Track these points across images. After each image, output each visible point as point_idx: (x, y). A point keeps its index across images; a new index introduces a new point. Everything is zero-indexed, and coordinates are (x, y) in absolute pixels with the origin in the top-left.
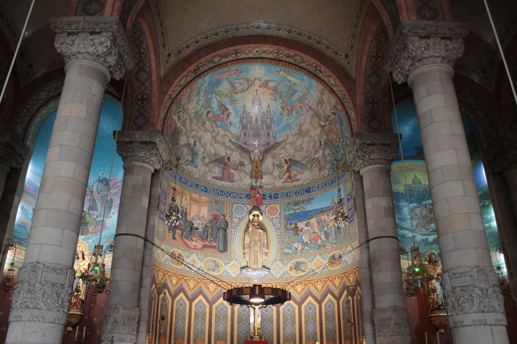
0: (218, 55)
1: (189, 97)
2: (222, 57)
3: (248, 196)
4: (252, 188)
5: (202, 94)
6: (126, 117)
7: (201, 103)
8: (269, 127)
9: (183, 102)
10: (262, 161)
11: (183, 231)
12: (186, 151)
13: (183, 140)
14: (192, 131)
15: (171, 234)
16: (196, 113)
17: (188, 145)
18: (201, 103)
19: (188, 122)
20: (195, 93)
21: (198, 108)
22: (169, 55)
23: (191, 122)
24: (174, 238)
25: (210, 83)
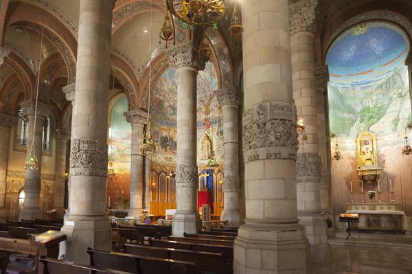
0: (162, 62)
1: (161, 84)
2: (165, 62)
3: (204, 124)
4: (206, 120)
5: (168, 80)
6: (129, 105)
7: (170, 84)
8: (208, 86)
9: (159, 87)
10: (209, 105)
11: (171, 147)
12: (169, 109)
13: (166, 105)
14: (170, 99)
15: (164, 149)
16: (170, 89)
17: (170, 106)
18: (170, 84)
19: (167, 95)
20: (164, 81)
21: (170, 87)
22: (139, 70)
23: (169, 95)
24: (166, 151)
25: (169, 74)
